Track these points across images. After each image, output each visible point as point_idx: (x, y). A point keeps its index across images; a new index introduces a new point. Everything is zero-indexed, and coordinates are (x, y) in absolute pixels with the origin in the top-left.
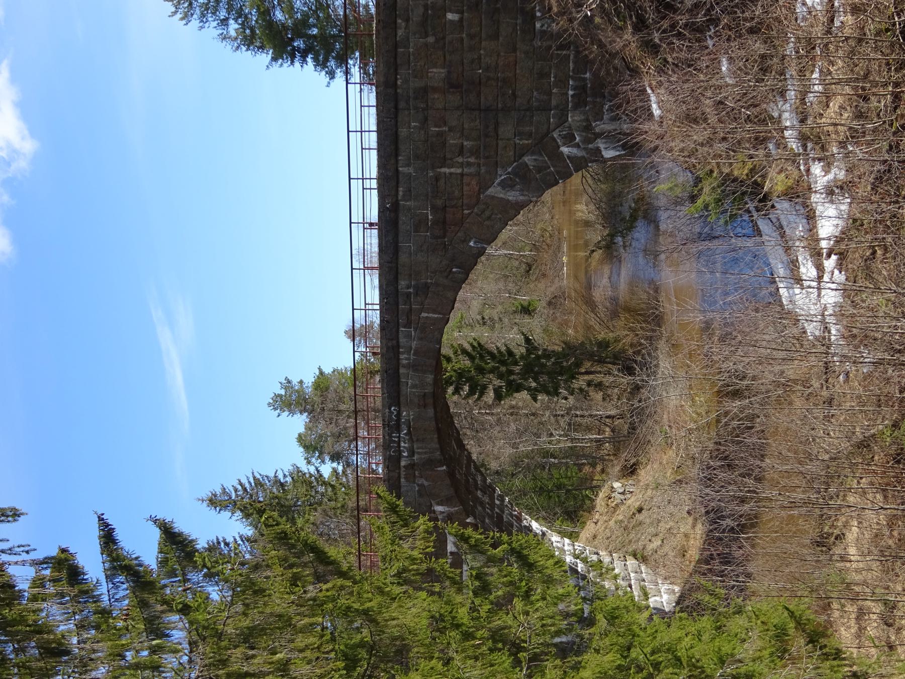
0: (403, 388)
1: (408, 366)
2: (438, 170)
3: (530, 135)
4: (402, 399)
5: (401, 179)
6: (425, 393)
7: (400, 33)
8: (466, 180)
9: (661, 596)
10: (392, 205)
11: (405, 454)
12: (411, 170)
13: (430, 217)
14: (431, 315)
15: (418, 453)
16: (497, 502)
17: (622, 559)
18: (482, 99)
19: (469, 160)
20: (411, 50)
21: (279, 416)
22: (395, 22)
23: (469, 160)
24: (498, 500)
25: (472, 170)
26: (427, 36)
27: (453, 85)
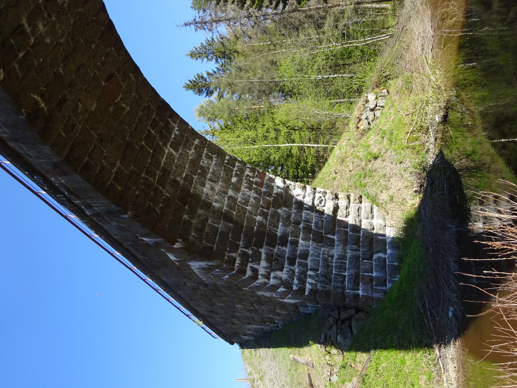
9: (385, 252)
16: (234, 180)
17: (358, 201)
24: (236, 175)
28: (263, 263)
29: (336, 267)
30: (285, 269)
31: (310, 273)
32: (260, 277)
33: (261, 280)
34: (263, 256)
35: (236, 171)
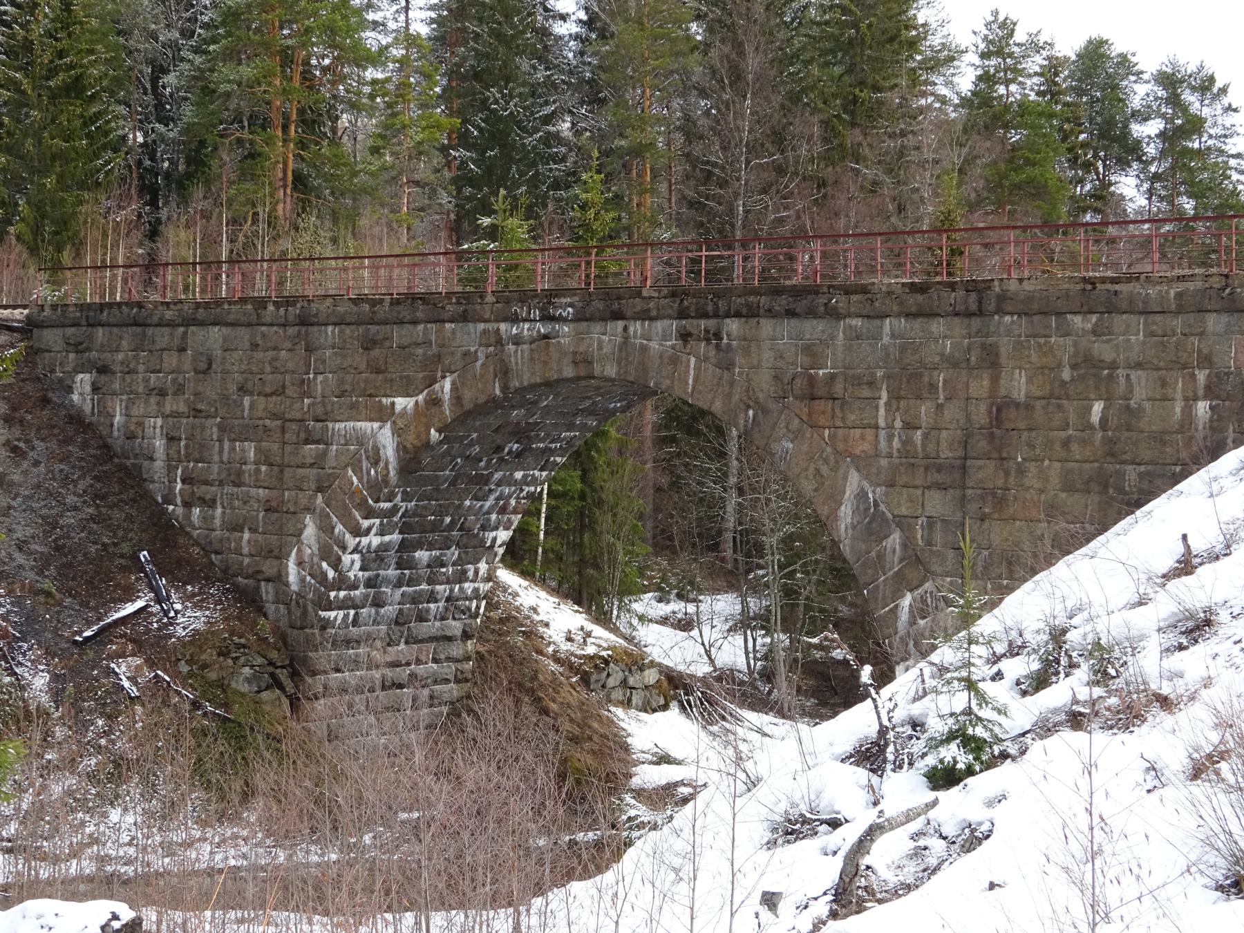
0: (597, 327)
1: (626, 338)
2: (884, 387)
3: (929, 543)
4: (585, 324)
5: (878, 322)
6: (590, 363)
7: (1077, 320)
8: (869, 433)
10: (835, 308)
11: (514, 331)
12: (886, 340)
13: (821, 372)
14: (692, 372)
15: (516, 351)
16: (519, 475)
18: (980, 462)
19: (896, 439)
20: (1053, 340)
21: (975, 33)
22: (1091, 312)
23: (896, 439)
25: (883, 444)
26: (1074, 367)
27: (1001, 408)
28: (375, 541)
29: (357, 655)
30: (361, 573)
31: (352, 612)
32: (358, 539)
33: (351, 542)
34: (387, 538)
35: (533, 475)
